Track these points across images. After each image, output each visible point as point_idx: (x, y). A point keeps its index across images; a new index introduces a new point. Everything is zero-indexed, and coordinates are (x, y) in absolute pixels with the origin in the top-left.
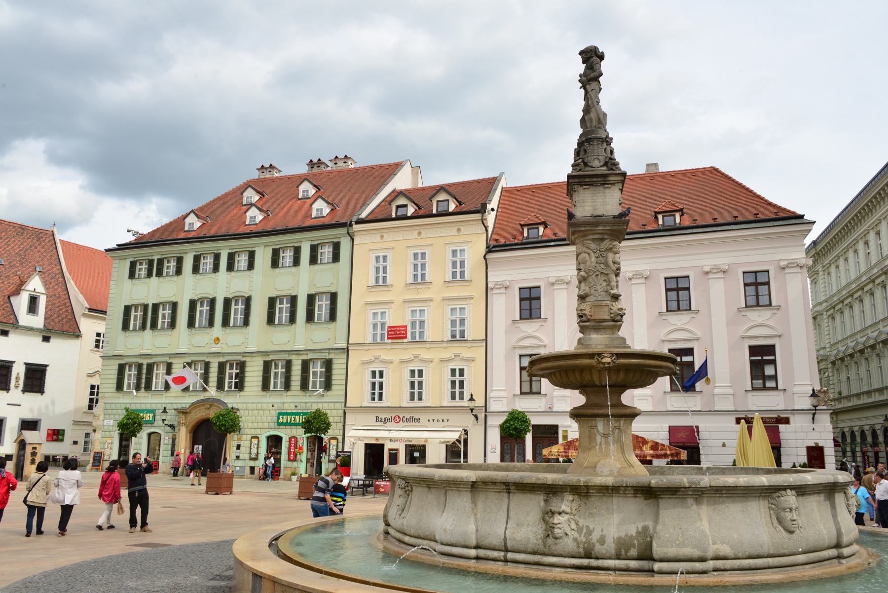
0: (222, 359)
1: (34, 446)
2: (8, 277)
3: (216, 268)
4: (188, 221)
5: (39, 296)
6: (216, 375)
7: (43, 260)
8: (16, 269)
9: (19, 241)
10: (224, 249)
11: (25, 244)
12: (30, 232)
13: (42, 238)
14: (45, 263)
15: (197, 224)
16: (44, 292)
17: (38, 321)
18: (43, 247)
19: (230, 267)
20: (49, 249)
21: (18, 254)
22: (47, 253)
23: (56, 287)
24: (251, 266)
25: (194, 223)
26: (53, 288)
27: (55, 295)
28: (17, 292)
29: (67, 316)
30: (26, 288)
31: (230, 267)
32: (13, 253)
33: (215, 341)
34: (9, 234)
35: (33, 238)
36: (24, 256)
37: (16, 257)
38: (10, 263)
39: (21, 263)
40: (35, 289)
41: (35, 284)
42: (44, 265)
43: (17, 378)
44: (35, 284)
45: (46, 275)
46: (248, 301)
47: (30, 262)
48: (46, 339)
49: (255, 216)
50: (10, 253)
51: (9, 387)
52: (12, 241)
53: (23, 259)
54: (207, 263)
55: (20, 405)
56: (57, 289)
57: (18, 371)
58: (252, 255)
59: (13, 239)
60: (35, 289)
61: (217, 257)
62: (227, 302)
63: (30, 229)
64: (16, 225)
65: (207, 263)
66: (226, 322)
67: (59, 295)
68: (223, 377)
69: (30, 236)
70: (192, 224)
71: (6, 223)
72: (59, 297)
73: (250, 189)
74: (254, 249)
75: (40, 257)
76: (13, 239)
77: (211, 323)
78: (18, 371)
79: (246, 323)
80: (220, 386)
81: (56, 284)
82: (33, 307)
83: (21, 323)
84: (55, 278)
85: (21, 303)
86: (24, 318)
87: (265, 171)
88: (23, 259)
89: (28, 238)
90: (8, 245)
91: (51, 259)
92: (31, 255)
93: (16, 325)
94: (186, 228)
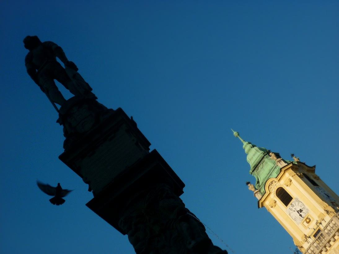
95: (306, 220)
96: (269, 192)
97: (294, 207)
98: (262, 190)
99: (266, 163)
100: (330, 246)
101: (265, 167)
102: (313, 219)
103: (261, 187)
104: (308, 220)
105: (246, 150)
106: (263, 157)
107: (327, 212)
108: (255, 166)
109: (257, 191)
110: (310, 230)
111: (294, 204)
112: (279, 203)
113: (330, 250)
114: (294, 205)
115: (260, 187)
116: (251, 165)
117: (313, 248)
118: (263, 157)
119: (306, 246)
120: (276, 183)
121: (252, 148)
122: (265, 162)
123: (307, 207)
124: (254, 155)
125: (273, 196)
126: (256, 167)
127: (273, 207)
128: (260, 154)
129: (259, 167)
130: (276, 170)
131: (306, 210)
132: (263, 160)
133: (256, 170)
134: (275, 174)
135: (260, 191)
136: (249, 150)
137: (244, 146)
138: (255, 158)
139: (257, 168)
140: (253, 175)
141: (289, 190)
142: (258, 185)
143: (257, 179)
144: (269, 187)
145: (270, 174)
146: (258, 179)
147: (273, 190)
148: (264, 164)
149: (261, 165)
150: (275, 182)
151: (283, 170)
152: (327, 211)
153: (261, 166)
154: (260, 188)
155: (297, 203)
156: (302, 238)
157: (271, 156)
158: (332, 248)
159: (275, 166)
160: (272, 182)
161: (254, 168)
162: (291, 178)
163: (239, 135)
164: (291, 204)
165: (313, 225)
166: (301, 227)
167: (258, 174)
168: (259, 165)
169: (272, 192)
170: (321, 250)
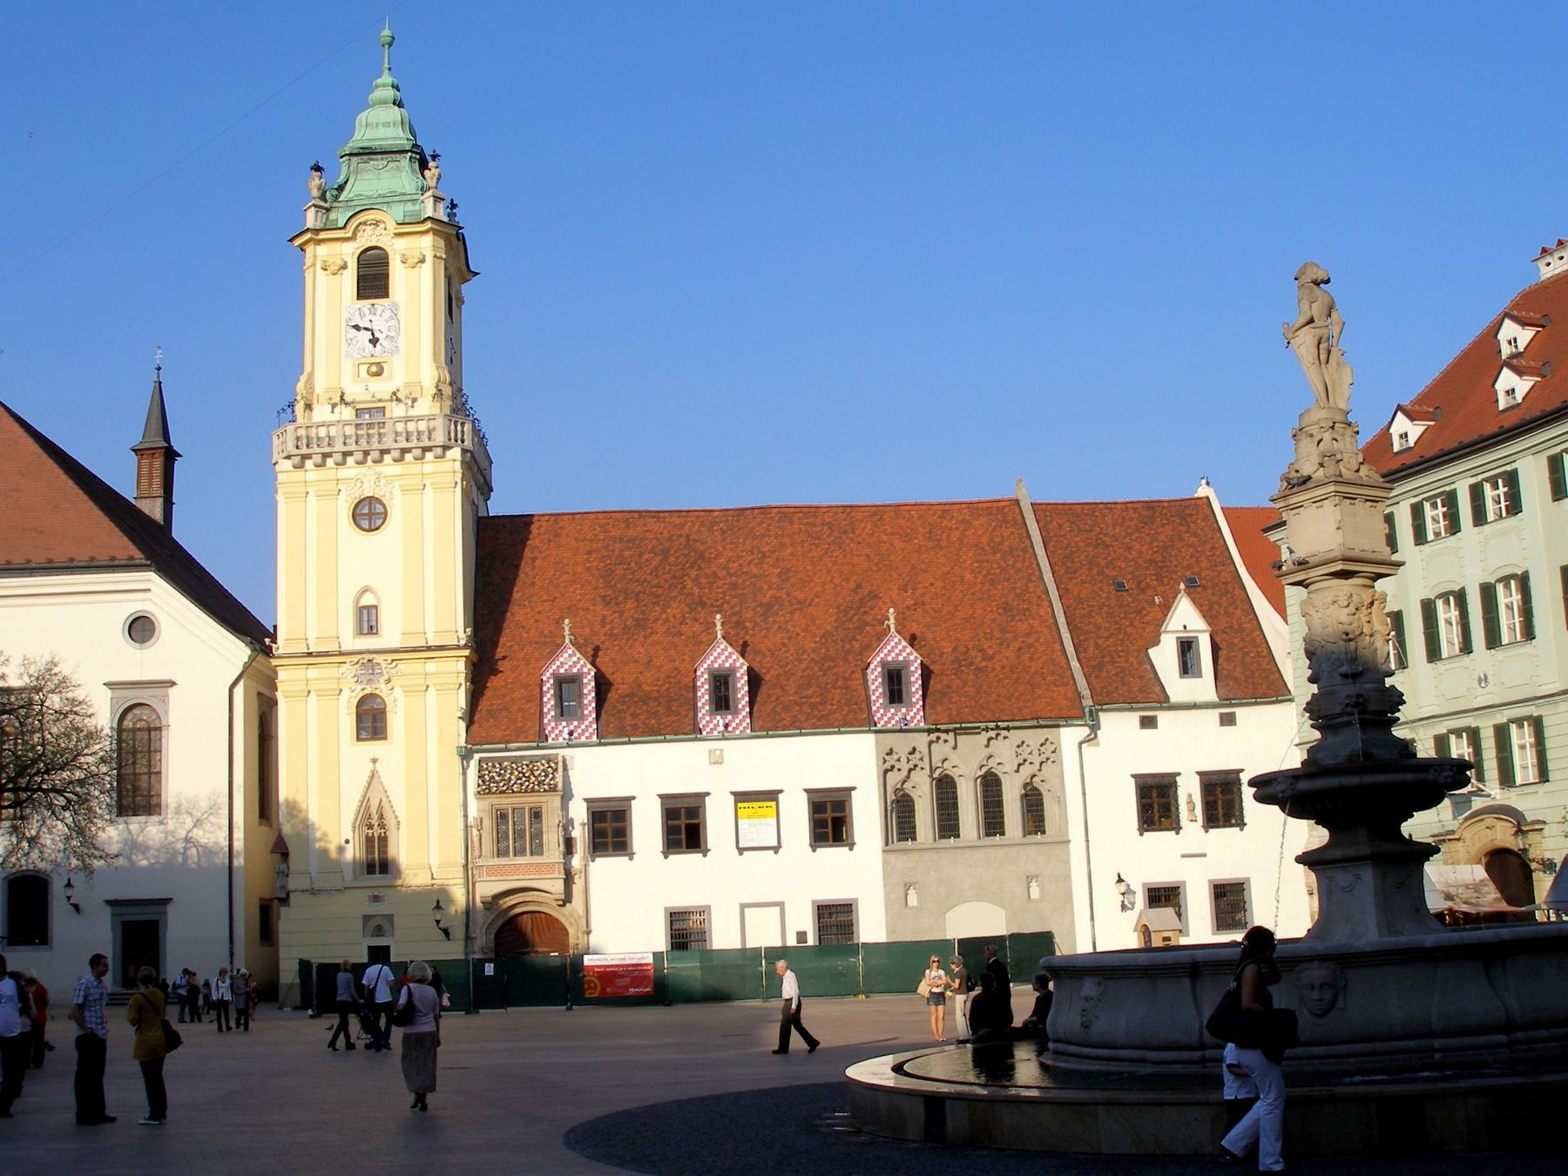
0: (1501, 718)
1: (1166, 934)
2: (1139, 612)
3: (1454, 526)
4: (1395, 431)
5: (1197, 637)
6: (1494, 755)
7: (1198, 561)
8: (1150, 592)
9: (1147, 535)
10: (1460, 479)
11: (1161, 538)
12: (1165, 511)
13: (1191, 515)
14: (1203, 565)
15: (1415, 430)
16: (1205, 628)
17: (1204, 687)
18: (1195, 535)
19: (1479, 518)
20: (1206, 536)
21: (1151, 561)
22: (1204, 543)
23: (1231, 610)
24: (1514, 506)
25: (1407, 431)
26: (1226, 613)
27: (1231, 627)
28: (1156, 641)
29: (1260, 665)
30: (1168, 629)
31: (1479, 518)
32: (1140, 561)
33: (1480, 681)
34: (1129, 527)
35: (1174, 521)
36: (1163, 562)
37: (1147, 568)
38: (1139, 583)
39: (1160, 578)
40: (1185, 627)
41: (1185, 616)
42: (1202, 570)
43: (1190, 802)
44: (1185, 616)
45: (1210, 592)
46: (1524, 581)
47: (1175, 572)
48: (1227, 720)
49: (1512, 386)
50: (1136, 563)
51: (1178, 823)
52: (1137, 538)
53: (1162, 568)
54: (1434, 516)
55: (1204, 855)
56: (1233, 613)
57: (1189, 791)
58: (1512, 479)
59: (1137, 534)
60: (1185, 627)
61: (1450, 499)
62: (1488, 592)
63: (1166, 505)
64: (1139, 506)
65: (1434, 516)
66: (1493, 640)
67: (1240, 625)
68: (1507, 757)
69: (1167, 519)
70: (1404, 436)
71: (1118, 506)
72: (1241, 630)
73: (1507, 323)
74: (1514, 466)
75: (1191, 557)
76: (1137, 534)
77: (1466, 648)
78: (1189, 791)
79: (1529, 633)
80: (1507, 778)
81: (1231, 604)
82: (1187, 666)
83: (1174, 699)
84: (1227, 592)
85: (1164, 657)
86: (1177, 687)
87: (1549, 259)
88: (1162, 568)
89: (1163, 526)
90: (1131, 548)
91: (1213, 555)
92: (1176, 556)
93: (1164, 702)
94: (1396, 448)
95: (372, 364)
96: (349, 235)
97: (372, 317)
98: (340, 217)
99: (398, 169)
100: (378, 461)
101: (385, 174)
102: (390, 378)
103: (339, 205)
104: (374, 369)
105: (378, 94)
106: (406, 152)
107: (439, 394)
108: (367, 151)
109: (322, 204)
110: (360, 390)
111: (379, 309)
112: (350, 277)
113: (369, 467)
114: (379, 312)
115: (335, 201)
116: (358, 136)
117: (337, 432)
118: (406, 152)
119: (321, 413)
120: (383, 232)
121: (394, 104)
122: (397, 163)
123: (402, 341)
124: (386, 125)
125: (349, 252)
126: (367, 153)
127: (328, 272)
128: (397, 136)
129: (372, 159)
130: (409, 207)
131: (393, 348)
132: (398, 156)
133: (360, 158)
134: (399, 212)
135: (328, 210)
136: (383, 102)
137: (379, 81)
138: (381, 133)
139: (365, 157)
140: (341, 160)
141: (398, 275)
142: (335, 193)
143: (341, 180)
144: (360, 224)
145: (387, 200)
146: (346, 182)
147: (363, 240)
148: (391, 164)
149: (382, 159)
150: (385, 229)
151: (429, 225)
152: (440, 390)
153: (379, 162)
154: (335, 204)
155: (387, 314)
156: (327, 390)
157: (430, 170)
158: (378, 468)
159: (415, 197)
160: (377, 223)
161: (361, 151)
162: (429, 259)
163: (390, 45)
164: (373, 305)
165: (382, 388)
166: (348, 367)
167: (357, 172)
168: (379, 157)
169: (358, 241)
170: (352, 452)
